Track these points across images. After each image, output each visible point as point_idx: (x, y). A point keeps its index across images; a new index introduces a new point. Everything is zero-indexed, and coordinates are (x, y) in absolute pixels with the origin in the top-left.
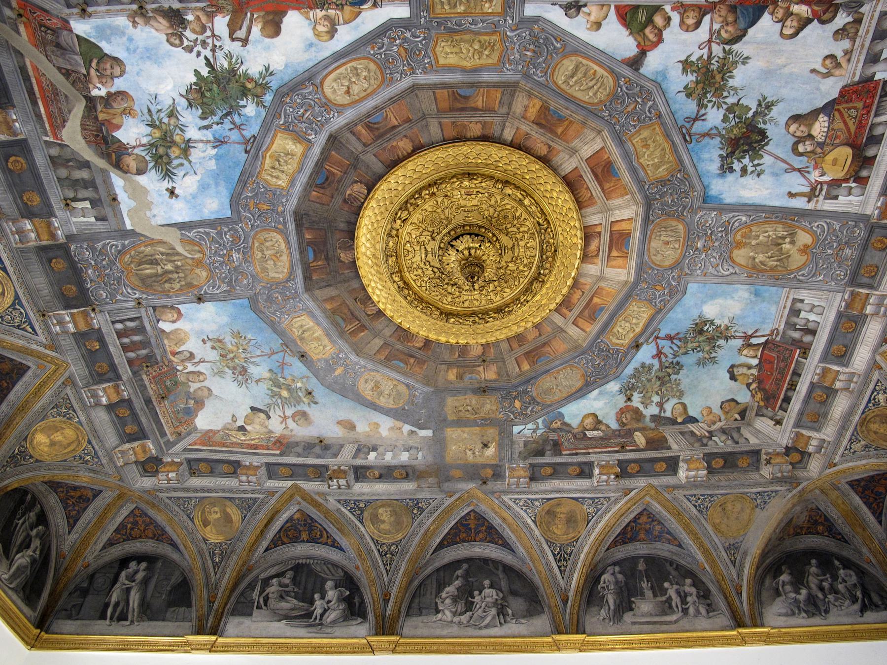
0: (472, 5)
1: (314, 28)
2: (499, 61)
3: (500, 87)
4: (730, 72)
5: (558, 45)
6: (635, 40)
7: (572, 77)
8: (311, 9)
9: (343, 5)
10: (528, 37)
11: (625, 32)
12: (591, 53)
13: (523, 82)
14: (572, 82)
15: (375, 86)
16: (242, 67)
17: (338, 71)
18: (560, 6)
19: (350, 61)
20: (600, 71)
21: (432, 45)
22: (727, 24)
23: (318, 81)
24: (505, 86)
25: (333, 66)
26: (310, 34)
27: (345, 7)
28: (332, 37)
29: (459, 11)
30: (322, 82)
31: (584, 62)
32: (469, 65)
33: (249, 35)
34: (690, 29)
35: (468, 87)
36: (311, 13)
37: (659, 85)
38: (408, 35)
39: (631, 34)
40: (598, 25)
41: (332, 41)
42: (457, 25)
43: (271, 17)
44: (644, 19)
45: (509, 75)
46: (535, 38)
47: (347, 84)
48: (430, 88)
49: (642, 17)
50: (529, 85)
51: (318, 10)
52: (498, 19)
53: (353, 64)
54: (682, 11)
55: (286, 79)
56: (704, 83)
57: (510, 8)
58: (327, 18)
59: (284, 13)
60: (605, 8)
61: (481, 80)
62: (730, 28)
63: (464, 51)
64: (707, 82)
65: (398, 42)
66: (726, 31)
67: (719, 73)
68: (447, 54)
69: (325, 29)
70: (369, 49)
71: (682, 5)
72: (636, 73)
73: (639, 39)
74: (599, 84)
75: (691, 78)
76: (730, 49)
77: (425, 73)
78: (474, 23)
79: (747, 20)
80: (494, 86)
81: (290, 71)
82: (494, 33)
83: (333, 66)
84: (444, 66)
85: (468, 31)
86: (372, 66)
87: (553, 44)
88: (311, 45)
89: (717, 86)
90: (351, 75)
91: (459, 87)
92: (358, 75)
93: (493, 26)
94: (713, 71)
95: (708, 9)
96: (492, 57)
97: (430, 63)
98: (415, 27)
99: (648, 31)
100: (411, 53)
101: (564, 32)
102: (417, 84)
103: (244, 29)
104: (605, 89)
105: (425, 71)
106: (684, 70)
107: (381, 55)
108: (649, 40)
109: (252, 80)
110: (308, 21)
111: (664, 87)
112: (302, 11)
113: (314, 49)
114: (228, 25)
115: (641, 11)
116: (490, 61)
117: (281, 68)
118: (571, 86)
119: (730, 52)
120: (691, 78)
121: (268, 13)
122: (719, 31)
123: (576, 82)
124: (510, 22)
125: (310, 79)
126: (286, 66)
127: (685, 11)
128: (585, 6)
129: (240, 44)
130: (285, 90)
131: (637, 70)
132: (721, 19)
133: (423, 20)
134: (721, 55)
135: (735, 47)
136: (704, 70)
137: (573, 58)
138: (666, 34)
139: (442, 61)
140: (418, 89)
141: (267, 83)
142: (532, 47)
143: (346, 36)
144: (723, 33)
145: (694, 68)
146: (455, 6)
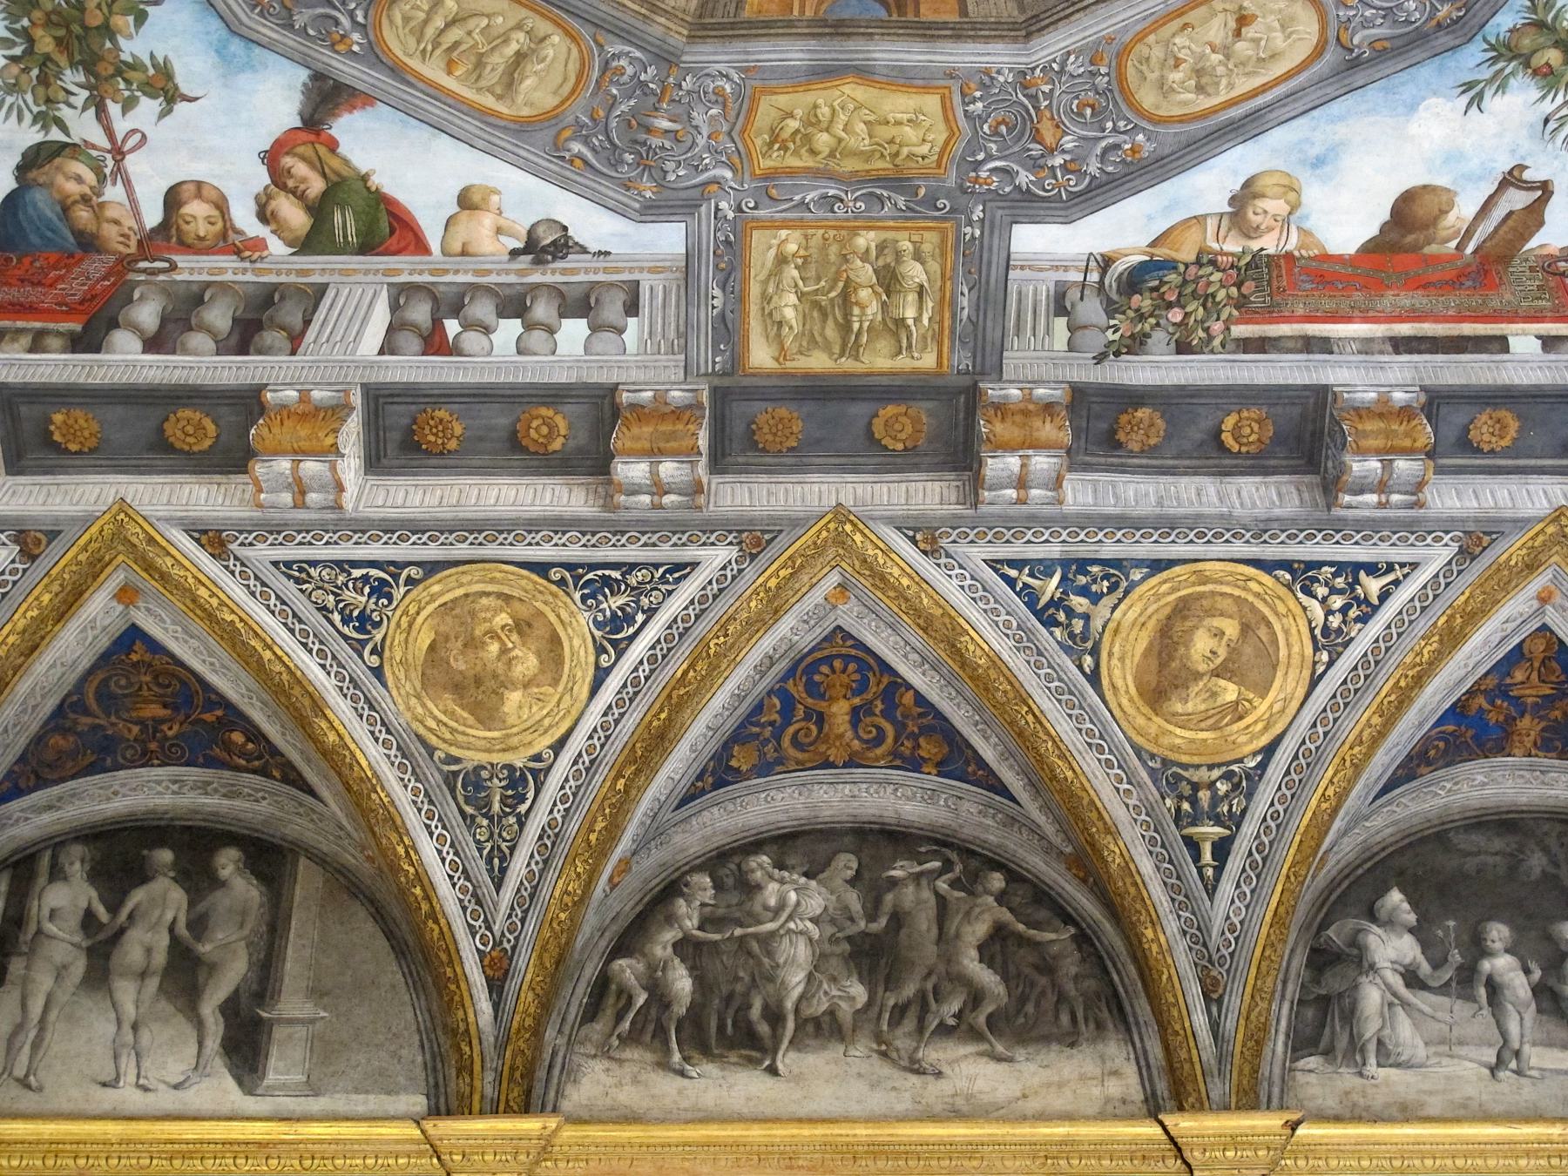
0: (834, 250)
1: (1294, 207)
2: (754, 101)
3: (751, 24)
4: (14, 59)
5: (577, 147)
6: (346, 162)
7: (520, 57)
8: (1289, 256)
9: (1199, 263)
10: (670, 166)
11: (384, 181)
12: (472, 125)
13: (677, 38)
14: (518, 41)
15: (1151, 38)
16: (1548, 107)
17: (1257, 82)
18: (584, 250)
19: (1214, 111)
20: (433, 71)
21: (958, 148)
22: (85, 200)
23: (1331, 56)
24: (733, 26)
25: (1269, 97)
26: (1314, 195)
27: (1192, 258)
28: (1247, 184)
29: (872, 234)
30: (1319, 51)
31: (489, 101)
32: (847, 89)
33: (1491, 197)
34: (192, 187)
35: (852, 23)
36: (1291, 245)
37: (233, 28)
38: (1024, 178)
39: (365, 178)
40: (467, 201)
41: (1252, 172)
42: (880, 198)
43: (1410, 238)
44: (338, 218)
45: (719, 60)
46: (648, 162)
47: (1240, 46)
48: (974, 26)
49: (344, 222)
50: (657, 31)
51: (1271, 251)
52: (761, 213)
53: (1206, 103)
54: (231, 236)
55: (1426, 72)
56: (86, 28)
57: (727, 242)
58: (1249, 232)
59: (1372, 248)
60: (457, 247)
61: (813, 44)
62: (72, 187)
63: (860, 128)
64: (76, 28)
65: (1058, 161)
66: (79, 179)
67: (47, 58)
68: (917, 124)
69: (1262, 204)
70: (1148, 147)
71: (238, 252)
72: (320, 67)
73: (335, 163)
74: (430, 32)
75: (135, 46)
76: (46, 128)
77: (987, 72)
78: (828, 202)
79: (30, 210)
80: (768, 24)
81: (1408, 92)
82: (770, 175)
83: (1269, 97)
84: (926, 89)
85: (851, 181)
86: (1148, 98)
87: (594, 150)
88: (1319, 162)
89: (37, 14)
90: (1221, 70)
91: (882, 24)
92: (1199, 72)
93: (774, 192)
94: (73, 65)
95: (159, 242)
96: (774, 113)
97: (967, 99)
98: (1004, 198)
99: (316, 186)
100: (1023, 127)
101: (565, 184)
102: (1015, 39)
103: (1498, 213)
104: (407, 19)
105: (986, 79)
106: (165, 72)
107: (1115, 130)
108: (303, 158)
109: (1535, 72)
110: (1307, 225)
111: (216, 24)
112: (1315, 252)
113: (1314, 151)
114: (1541, 223)
115: (353, 239)
116: (782, 100)
117: (1433, 101)
118: (519, 26)
119: (44, 120)
120: (135, 46)
121: (1415, 248)
122: (102, 179)
123: (506, 41)
124: (723, 205)
125: (1354, 64)
126: (1412, 107)
127: (224, 235)
128: (514, 253)
129: (1527, 175)
130: (1445, 40)
131: (318, 77)
132: (110, 213)
133: (978, 214)
134: (65, 112)
135: (32, 136)
136: (105, 69)
137: (526, 112)
138: (262, 178)
139: (932, 103)
140: (1014, 26)
141: (1494, 60)
142: (655, 142)
143: (1207, 187)
144: (90, 177)
145: (131, 75)
146: (881, 248)
